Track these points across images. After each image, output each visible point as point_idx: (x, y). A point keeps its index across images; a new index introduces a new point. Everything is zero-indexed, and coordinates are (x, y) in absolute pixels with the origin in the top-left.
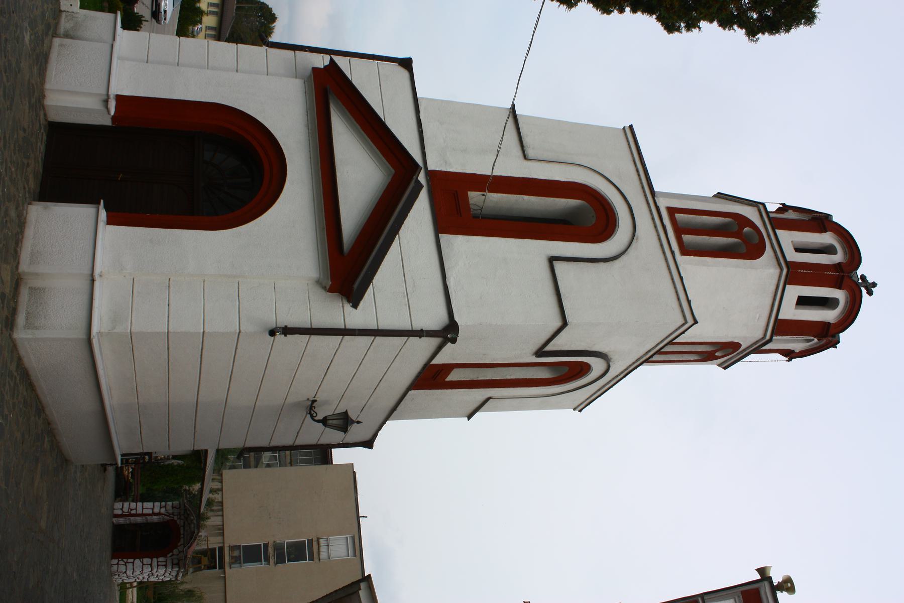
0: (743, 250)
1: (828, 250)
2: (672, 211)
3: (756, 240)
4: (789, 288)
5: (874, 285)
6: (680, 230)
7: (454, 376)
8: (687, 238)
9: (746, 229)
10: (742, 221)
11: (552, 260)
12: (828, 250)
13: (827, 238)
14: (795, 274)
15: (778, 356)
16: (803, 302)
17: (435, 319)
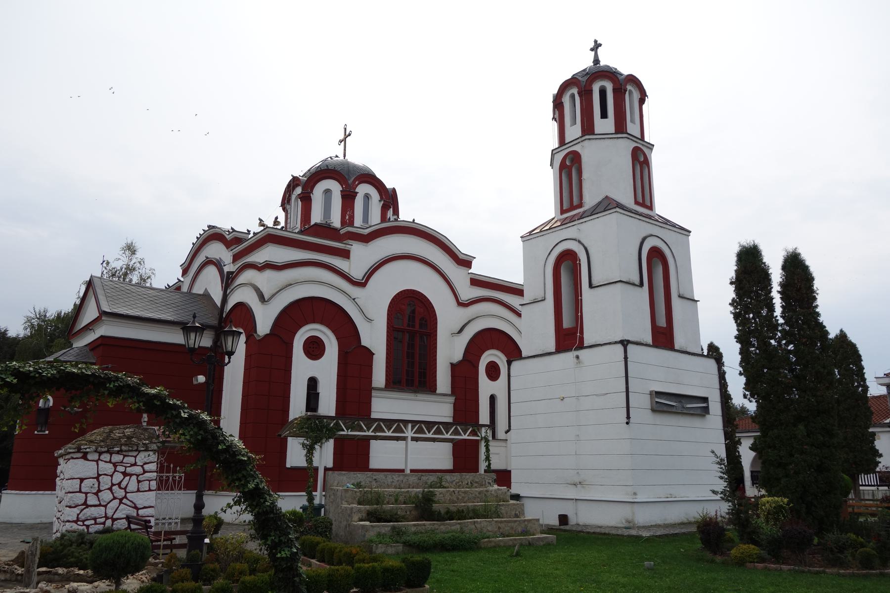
0: (577, 165)
1: (573, 96)
2: (563, 212)
3: (571, 156)
4: (597, 131)
5: (596, 41)
6: (572, 208)
7: (662, 322)
8: (576, 201)
9: (568, 163)
10: (563, 166)
11: (591, 286)
12: (573, 96)
13: (566, 100)
14: (588, 129)
15: (644, 107)
16: (604, 115)
17: (620, 348)
